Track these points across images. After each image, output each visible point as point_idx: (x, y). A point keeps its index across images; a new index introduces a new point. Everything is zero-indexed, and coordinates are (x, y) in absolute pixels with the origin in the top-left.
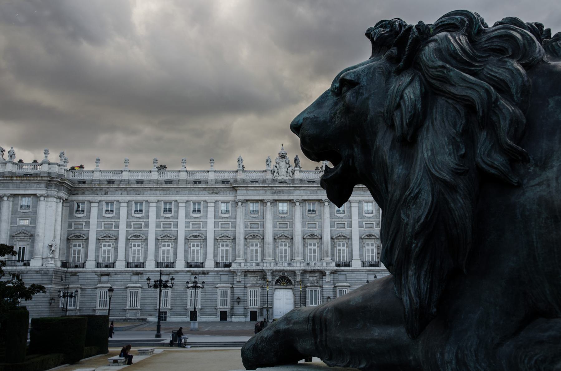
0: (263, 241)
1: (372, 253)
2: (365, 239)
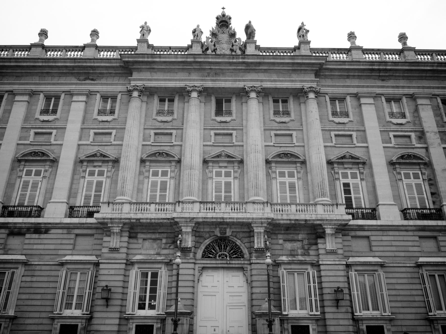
0: (180, 166)
1: (420, 192)
2: (400, 164)
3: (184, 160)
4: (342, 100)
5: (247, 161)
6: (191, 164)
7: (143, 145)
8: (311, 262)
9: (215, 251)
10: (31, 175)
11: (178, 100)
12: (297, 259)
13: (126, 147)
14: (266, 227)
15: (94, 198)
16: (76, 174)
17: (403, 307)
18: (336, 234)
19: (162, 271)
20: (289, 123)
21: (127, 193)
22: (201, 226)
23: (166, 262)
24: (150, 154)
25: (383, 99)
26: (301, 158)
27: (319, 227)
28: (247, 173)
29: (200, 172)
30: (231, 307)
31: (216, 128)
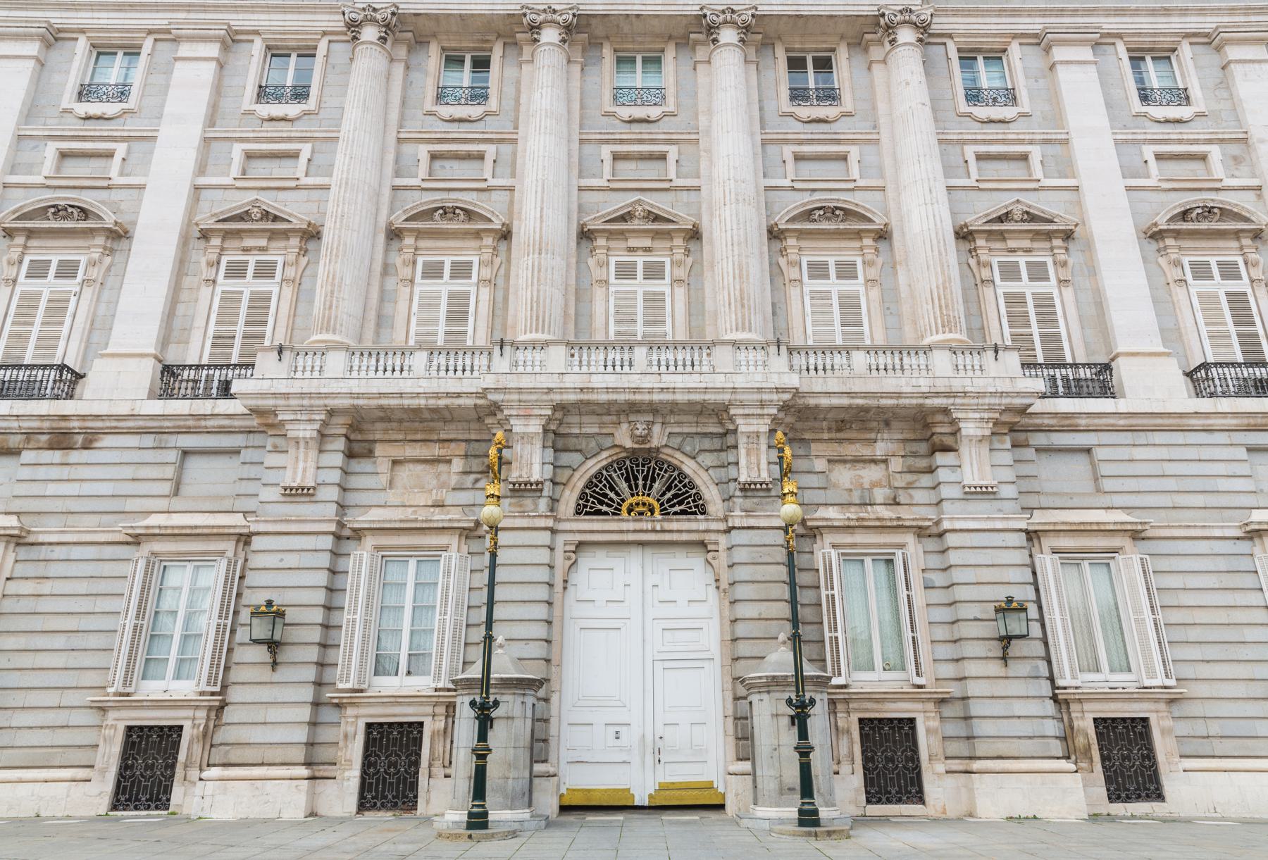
0: (509, 249)
2: (1178, 234)
3: (520, 229)
4: (996, 56)
5: (711, 233)
6: (541, 237)
7: (395, 188)
8: (914, 524)
9: (617, 494)
10: (45, 277)
11: (503, 57)
12: (872, 516)
13: (340, 187)
14: (775, 419)
15: (243, 343)
16: (187, 275)
17: (1208, 661)
18: (994, 438)
19: (450, 557)
20: (837, 123)
21: (341, 325)
22: (574, 419)
23: (464, 529)
24: (415, 211)
25: (1121, 48)
26: (878, 222)
27: (939, 417)
28: (712, 267)
29: (568, 265)
30: (667, 664)
31: (618, 136)
